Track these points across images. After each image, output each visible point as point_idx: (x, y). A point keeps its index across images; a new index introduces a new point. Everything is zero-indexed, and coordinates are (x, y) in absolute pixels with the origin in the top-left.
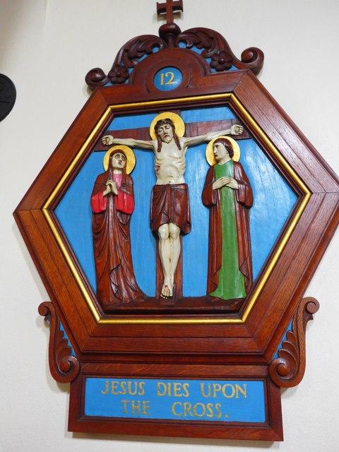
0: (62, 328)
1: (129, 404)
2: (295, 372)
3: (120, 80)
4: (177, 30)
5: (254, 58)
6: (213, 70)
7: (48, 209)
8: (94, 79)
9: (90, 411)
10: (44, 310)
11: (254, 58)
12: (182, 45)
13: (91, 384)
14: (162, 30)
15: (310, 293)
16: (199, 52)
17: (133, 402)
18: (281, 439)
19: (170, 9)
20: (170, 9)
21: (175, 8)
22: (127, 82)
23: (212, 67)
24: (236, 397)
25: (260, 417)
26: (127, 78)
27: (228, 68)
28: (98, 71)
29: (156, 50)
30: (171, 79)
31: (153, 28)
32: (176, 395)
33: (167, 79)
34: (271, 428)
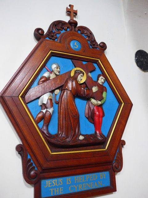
0: (29, 157)
1: (54, 191)
2: (118, 167)
3: (53, 38)
4: (76, 23)
5: (103, 46)
6: (91, 47)
7: (21, 97)
8: (39, 34)
9: (44, 194)
10: (20, 149)
11: (103, 46)
12: (79, 32)
13: (43, 182)
14: (70, 23)
15: (122, 139)
16: (85, 37)
17: (55, 189)
18: (116, 191)
19: (71, 12)
20: (71, 12)
21: (74, 13)
22: (56, 40)
23: (91, 46)
24: (99, 179)
25: (107, 184)
26: (56, 38)
27: (96, 48)
28: (38, 30)
29: (68, 30)
30: (75, 45)
31: (67, 19)
32: (80, 182)
33: (74, 45)
34: (112, 188)
